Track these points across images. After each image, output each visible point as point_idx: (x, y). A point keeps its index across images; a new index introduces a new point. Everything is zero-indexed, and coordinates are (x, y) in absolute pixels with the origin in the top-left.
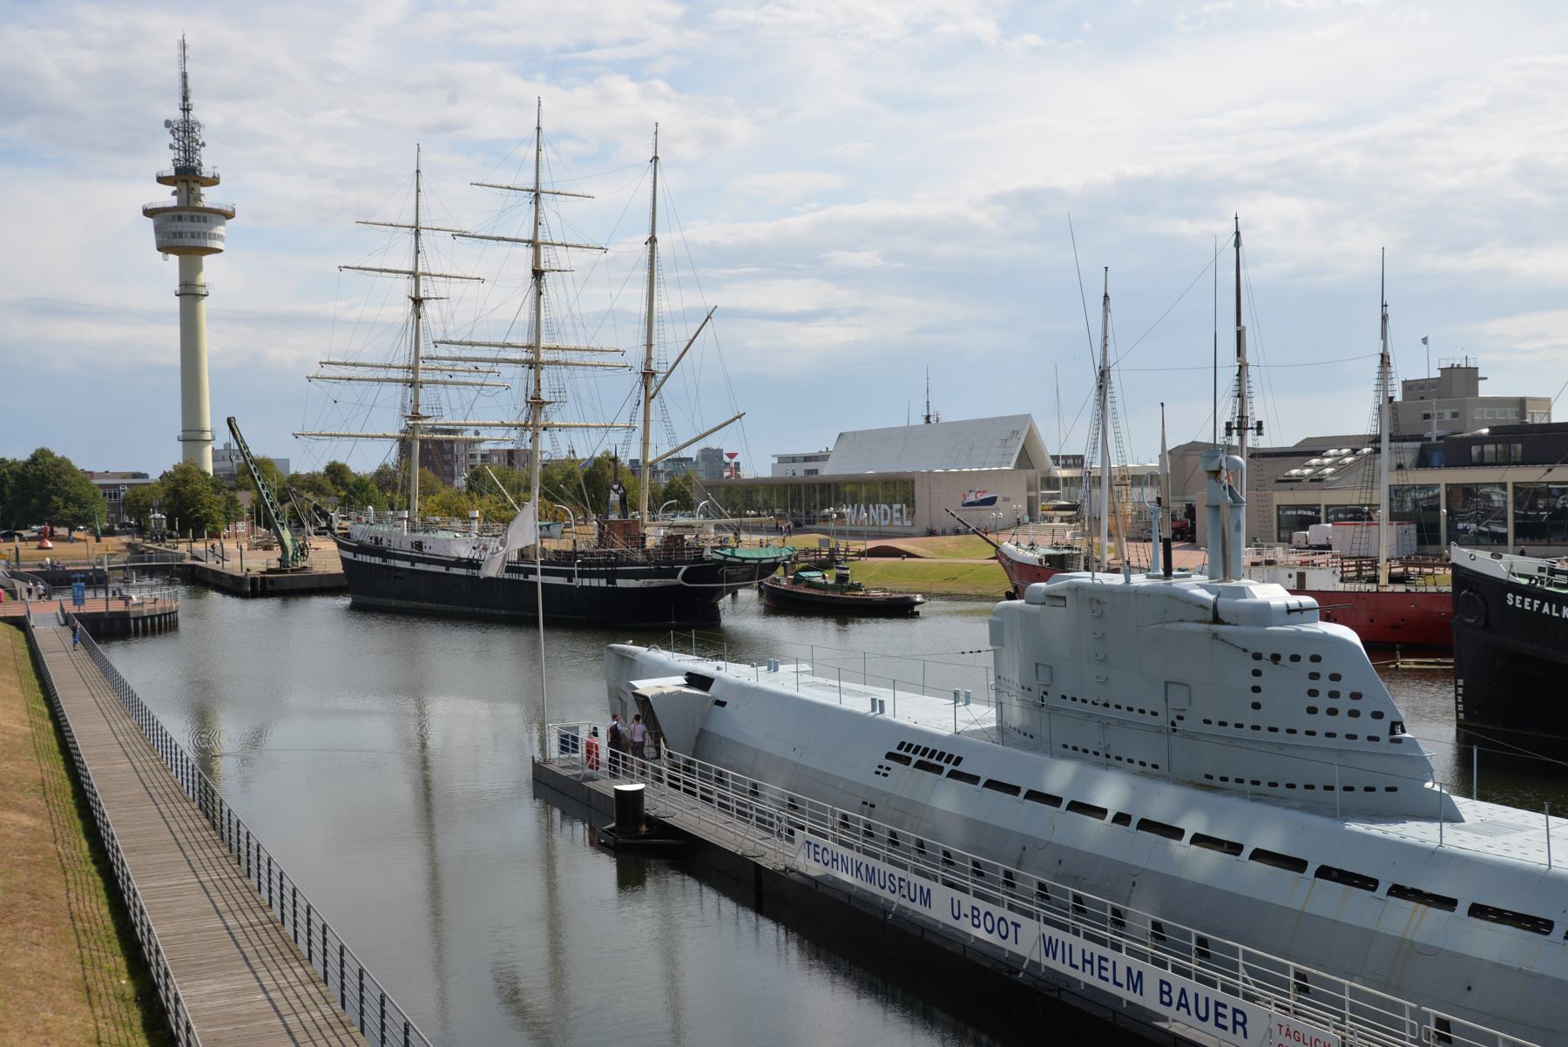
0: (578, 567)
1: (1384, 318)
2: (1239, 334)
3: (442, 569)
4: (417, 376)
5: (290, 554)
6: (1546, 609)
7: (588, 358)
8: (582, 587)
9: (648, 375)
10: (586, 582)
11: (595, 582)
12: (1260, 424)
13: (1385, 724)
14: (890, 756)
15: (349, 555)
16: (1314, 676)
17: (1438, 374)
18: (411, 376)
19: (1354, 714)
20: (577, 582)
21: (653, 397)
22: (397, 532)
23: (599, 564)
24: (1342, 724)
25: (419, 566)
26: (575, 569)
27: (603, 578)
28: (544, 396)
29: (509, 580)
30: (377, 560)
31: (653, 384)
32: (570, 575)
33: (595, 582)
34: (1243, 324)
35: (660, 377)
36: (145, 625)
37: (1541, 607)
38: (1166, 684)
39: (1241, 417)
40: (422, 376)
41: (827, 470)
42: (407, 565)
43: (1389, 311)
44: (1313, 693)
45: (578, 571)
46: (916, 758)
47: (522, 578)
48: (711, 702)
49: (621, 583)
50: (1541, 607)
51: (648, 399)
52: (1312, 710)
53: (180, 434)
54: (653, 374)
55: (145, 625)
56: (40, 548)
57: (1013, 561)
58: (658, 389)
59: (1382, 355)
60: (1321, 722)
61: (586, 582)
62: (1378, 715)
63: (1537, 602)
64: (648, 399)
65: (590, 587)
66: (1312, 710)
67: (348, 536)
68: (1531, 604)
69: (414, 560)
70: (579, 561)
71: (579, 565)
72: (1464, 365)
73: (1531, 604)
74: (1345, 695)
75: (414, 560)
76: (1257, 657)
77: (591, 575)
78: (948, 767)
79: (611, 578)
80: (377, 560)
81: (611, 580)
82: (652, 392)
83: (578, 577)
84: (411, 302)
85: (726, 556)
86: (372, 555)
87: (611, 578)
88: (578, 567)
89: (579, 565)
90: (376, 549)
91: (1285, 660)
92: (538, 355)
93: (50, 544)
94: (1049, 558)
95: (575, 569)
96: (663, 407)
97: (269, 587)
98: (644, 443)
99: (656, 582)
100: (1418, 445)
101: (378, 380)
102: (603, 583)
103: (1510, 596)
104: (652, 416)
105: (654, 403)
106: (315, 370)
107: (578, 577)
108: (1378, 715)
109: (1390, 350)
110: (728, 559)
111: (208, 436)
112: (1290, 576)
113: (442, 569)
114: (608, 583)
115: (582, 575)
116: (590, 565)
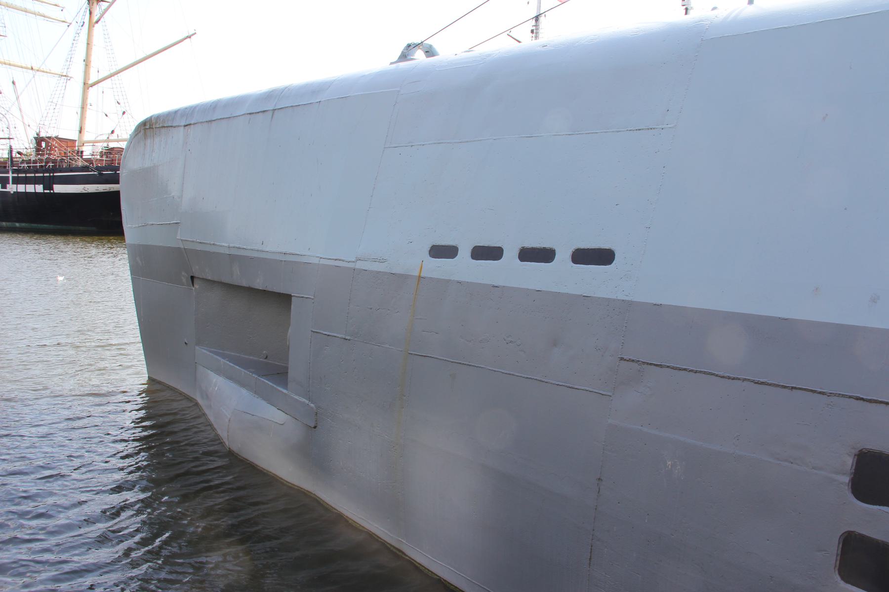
0: (13, 173)
10: (21, 188)
11: (30, 188)
21: (97, 22)
23: (36, 171)
26: (10, 175)
27: (39, 184)
33: (30, 188)
45: (13, 177)
49: (58, 189)
58: (102, 16)
61: (21, 188)
65: (26, 193)
70: (14, 168)
71: (14, 172)
77: (26, 181)
79: (48, 183)
82: (95, 19)
83: (13, 183)
87: (48, 183)
88: (13, 173)
98: (86, 65)
99: (92, 188)
102: (40, 188)
107: (13, 183)
114: (44, 189)
115: (16, 181)
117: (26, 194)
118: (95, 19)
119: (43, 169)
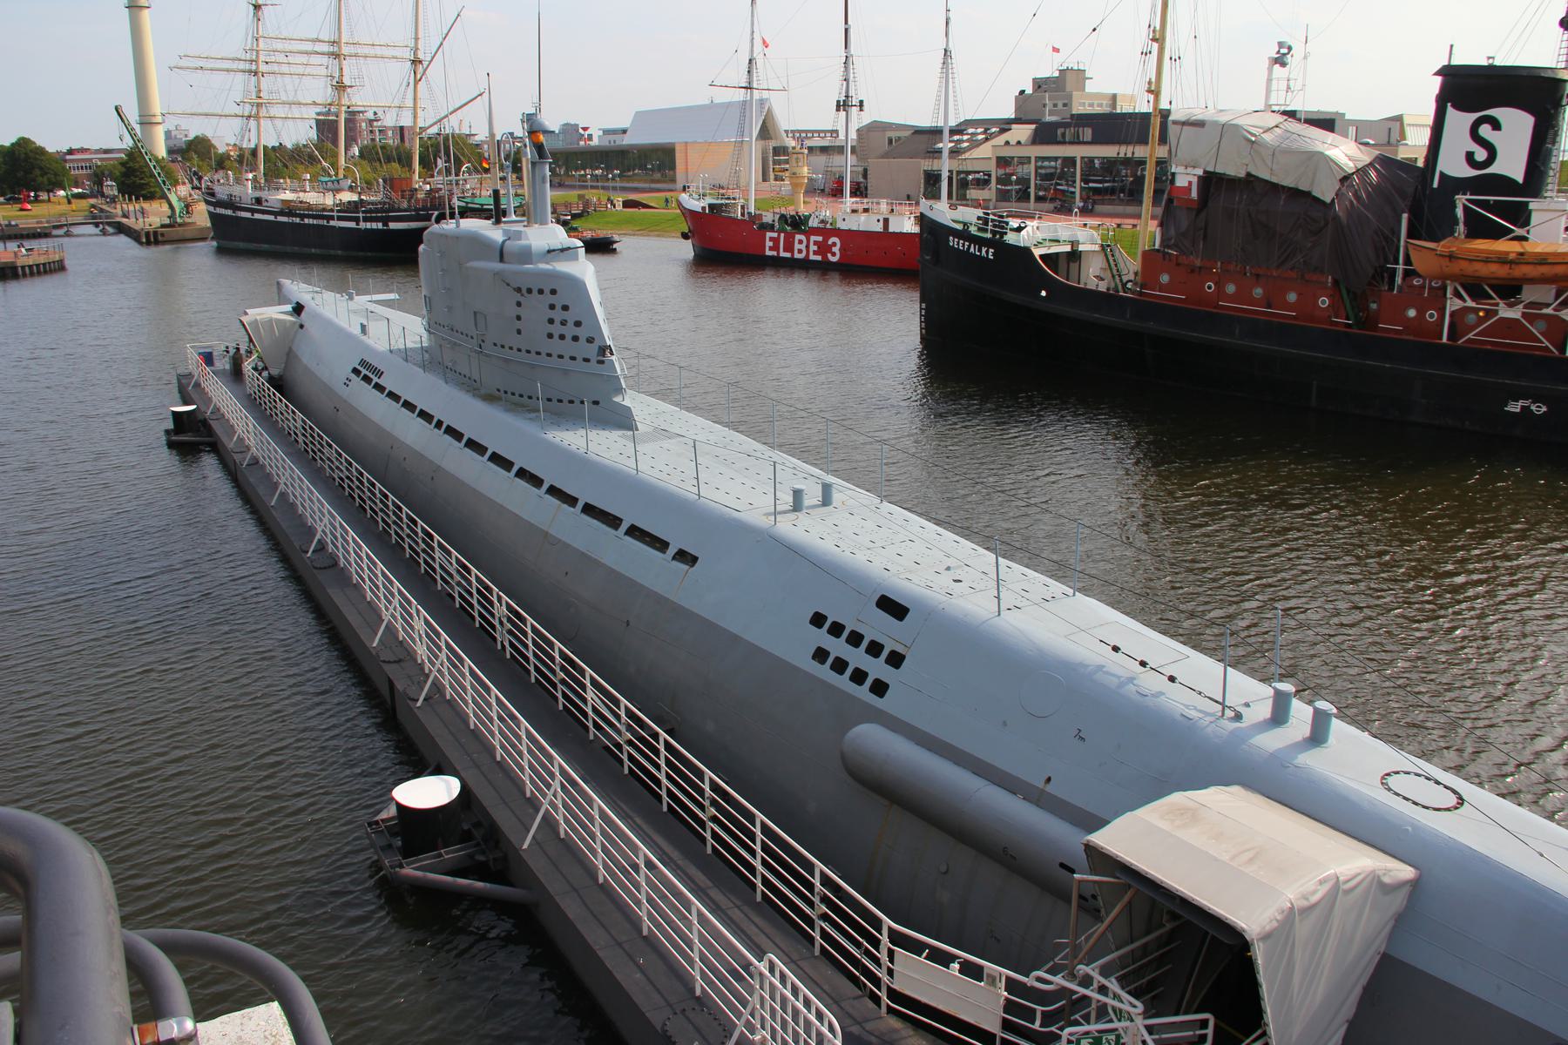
1: (947, 23)
2: (846, 30)
3: (271, 218)
4: (258, 67)
5: (178, 211)
6: (972, 250)
7: (378, 51)
8: (366, 229)
9: (416, 62)
10: (368, 225)
11: (374, 226)
12: (861, 102)
13: (594, 347)
14: (356, 371)
15: (211, 209)
16: (552, 307)
17: (1056, 74)
18: (254, 67)
19: (575, 339)
20: (363, 225)
22: (245, 188)
23: (377, 211)
24: (567, 348)
25: (257, 216)
26: (361, 215)
28: (347, 81)
29: (318, 226)
30: (229, 212)
31: (420, 69)
32: (357, 220)
33: (374, 226)
34: (849, 23)
35: (426, 64)
36: (45, 268)
37: (969, 247)
38: (475, 313)
39: (847, 97)
40: (263, 68)
41: (627, 140)
42: (248, 215)
43: (951, 15)
44: (551, 321)
46: (364, 372)
47: (325, 222)
48: (297, 326)
49: (393, 225)
50: (969, 247)
51: (417, 82)
52: (550, 336)
53: (138, 118)
54: (421, 62)
55: (45, 268)
56: (22, 210)
57: (685, 209)
58: (424, 73)
59: (946, 50)
60: (556, 346)
61: (368, 225)
62: (590, 340)
63: (967, 243)
64: (417, 82)
66: (550, 336)
67: (213, 195)
68: (964, 245)
69: (253, 211)
71: (363, 212)
72: (1076, 68)
73: (964, 245)
74: (570, 324)
75: (253, 211)
76: (519, 290)
78: (375, 380)
79: (385, 221)
80: (229, 212)
81: (385, 224)
82: (419, 77)
84: (252, 8)
85: (467, 203)
86: (226, 208)
87: (385, 221)
89: (363, 212)
90: (230, 204)
91: (535, 292)
92: (340, 48)
93: (29, 207)
94: (711, 206)
95: (361, 215)
96: (430, 89)
97: (160, 238)
100: (1033, 126)
101: (228, 71)
102: (380, 225)
103: (951, 238)
104: (419, 95)
105: (421, 85)
106: (176, 61)
108: (590, 340)
109: (951, 46)
110: (470, 205)
111: (159, 119)
112: (878, 221)
113: (271, 218)
115: (366, 220)
116: (374, 213)
117: (372, 230)
118: (419, 77)
119: (382, 211)
